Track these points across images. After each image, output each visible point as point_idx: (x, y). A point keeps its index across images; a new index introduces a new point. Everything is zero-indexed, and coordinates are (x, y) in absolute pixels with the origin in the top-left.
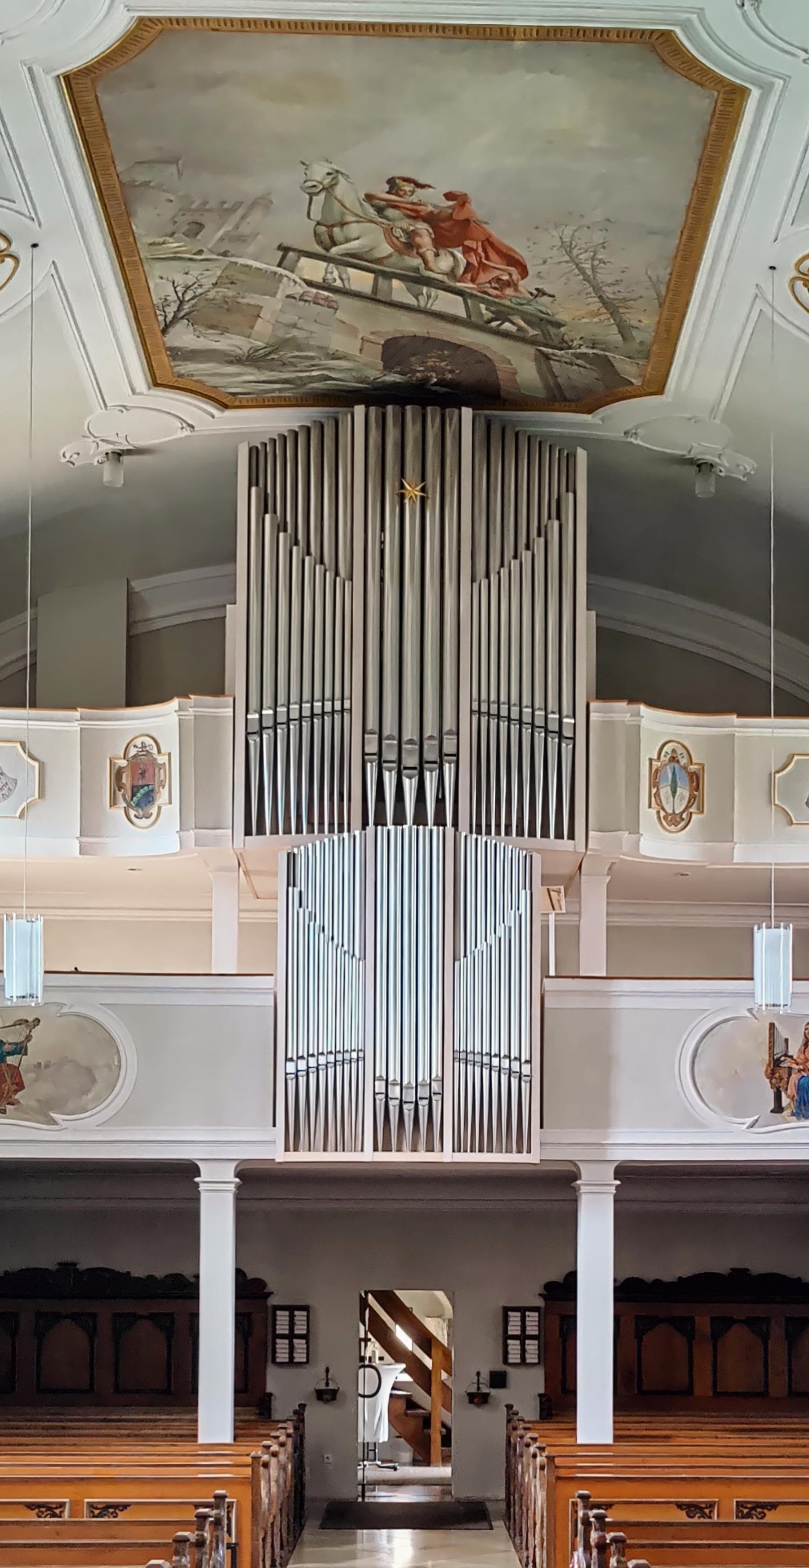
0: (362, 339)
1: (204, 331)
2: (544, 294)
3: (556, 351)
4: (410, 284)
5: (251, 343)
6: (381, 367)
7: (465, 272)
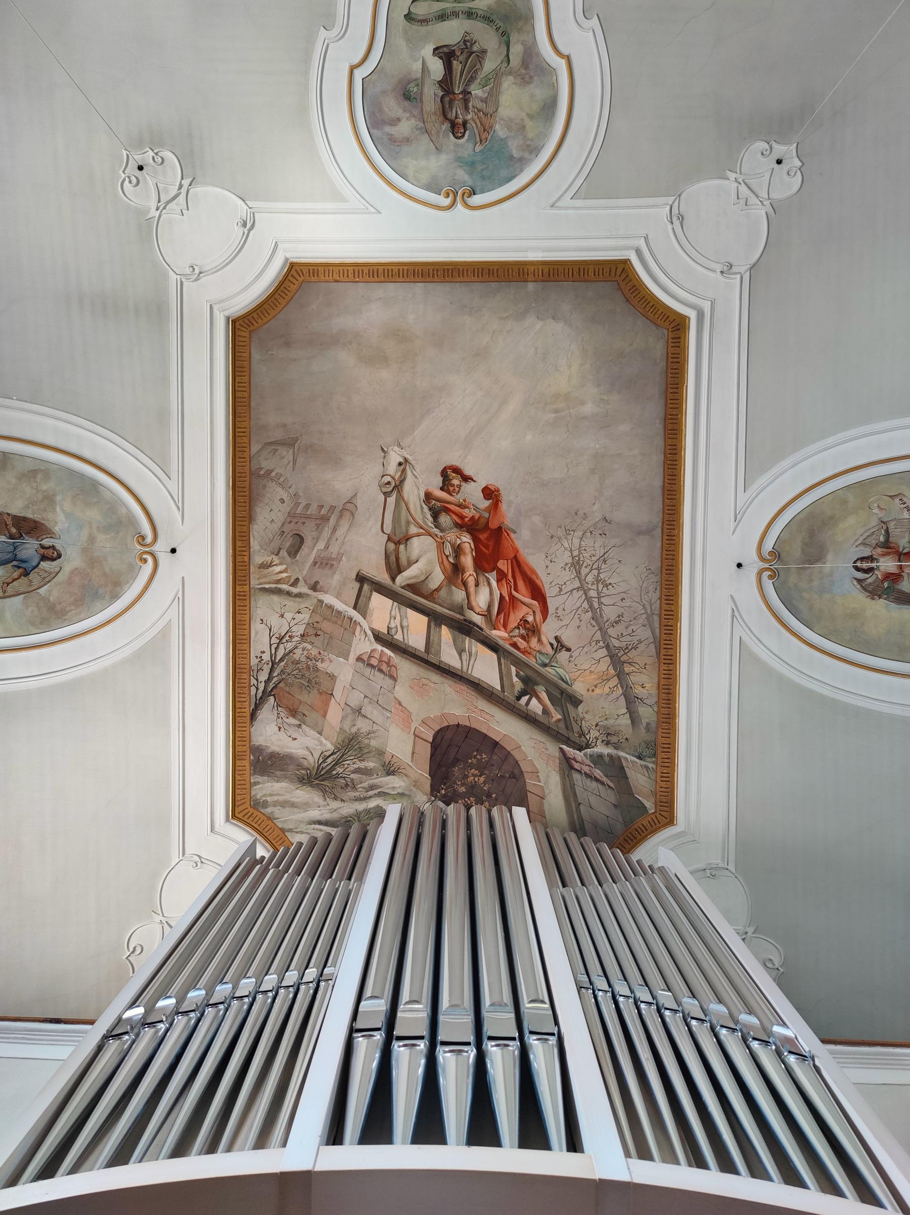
0: (415, 735)
1: (285, 719)
2: (563, 646)
3: (579, 755)
4: (457, 633)
5: (321, 744)
6: (428, 788)
7: (499, 613)
